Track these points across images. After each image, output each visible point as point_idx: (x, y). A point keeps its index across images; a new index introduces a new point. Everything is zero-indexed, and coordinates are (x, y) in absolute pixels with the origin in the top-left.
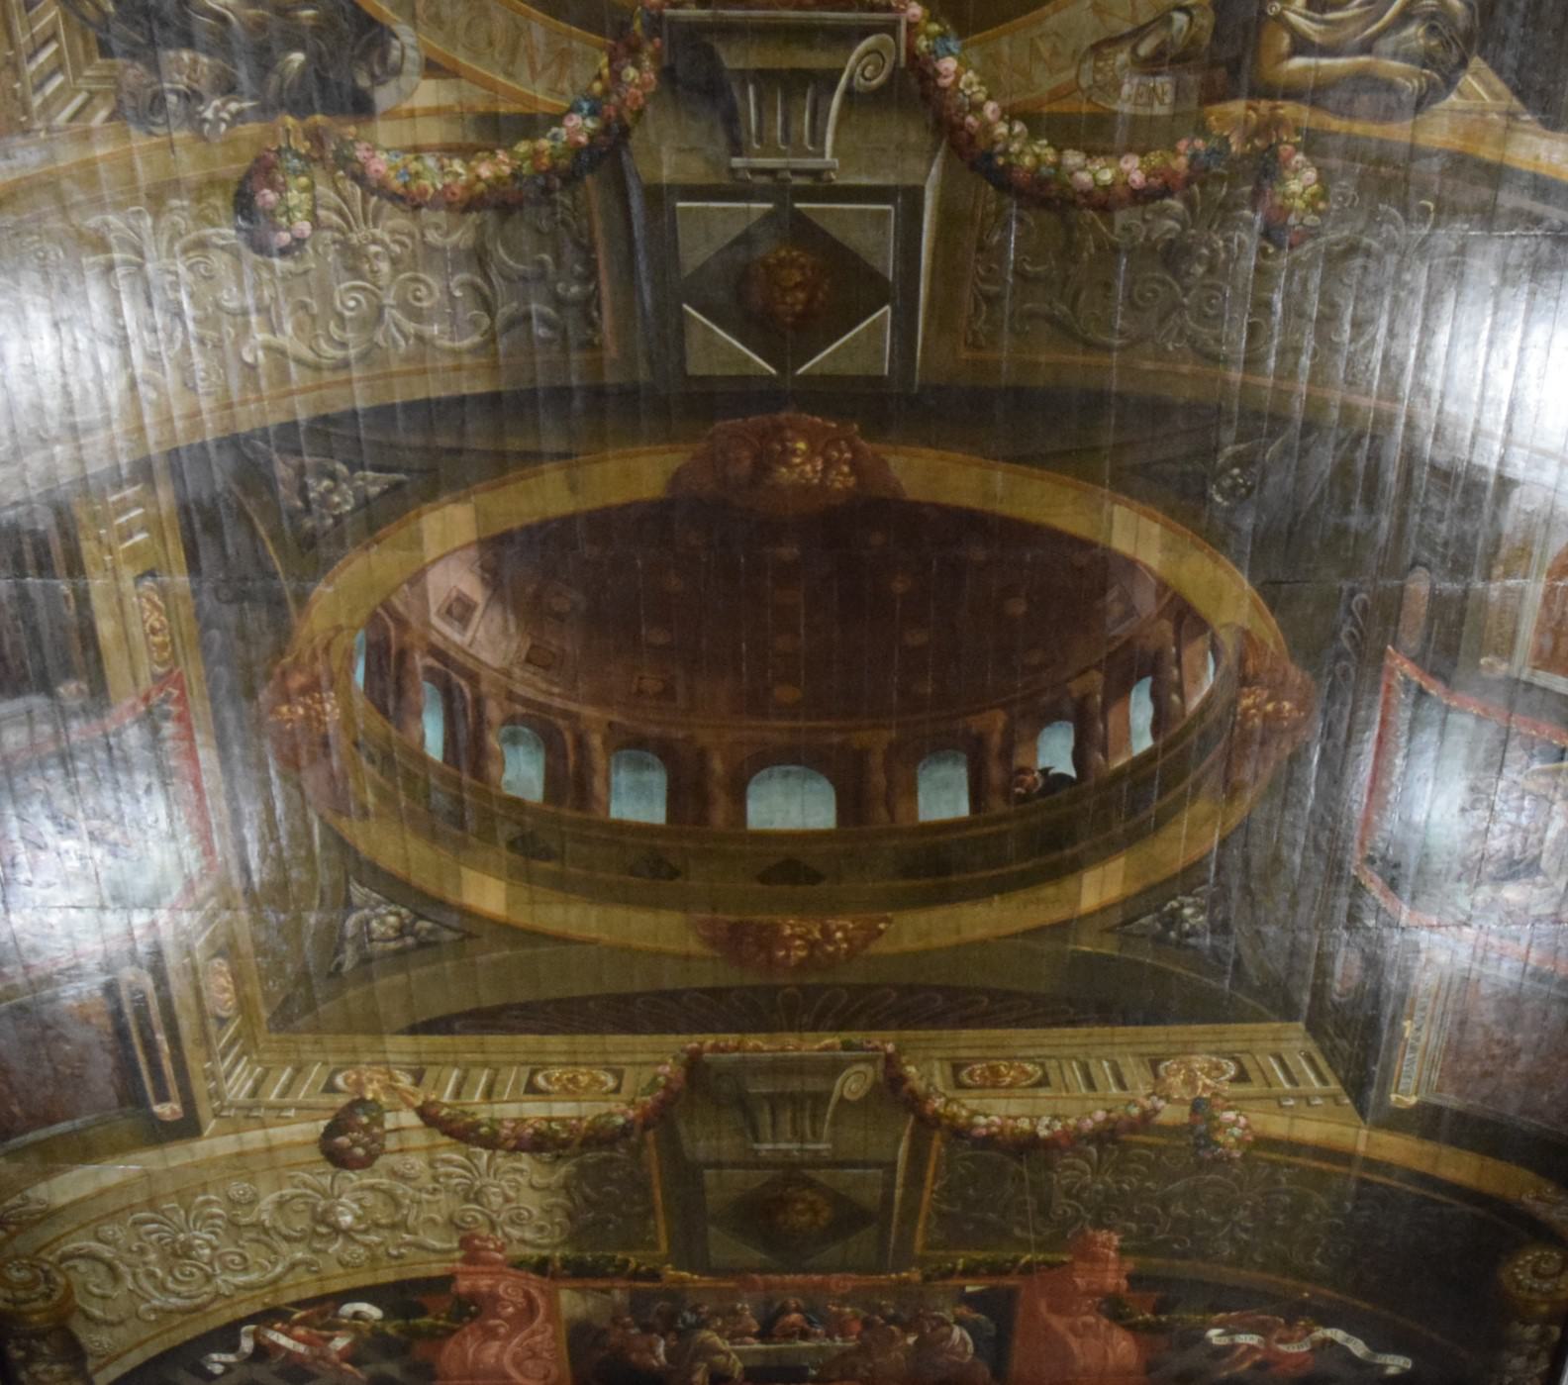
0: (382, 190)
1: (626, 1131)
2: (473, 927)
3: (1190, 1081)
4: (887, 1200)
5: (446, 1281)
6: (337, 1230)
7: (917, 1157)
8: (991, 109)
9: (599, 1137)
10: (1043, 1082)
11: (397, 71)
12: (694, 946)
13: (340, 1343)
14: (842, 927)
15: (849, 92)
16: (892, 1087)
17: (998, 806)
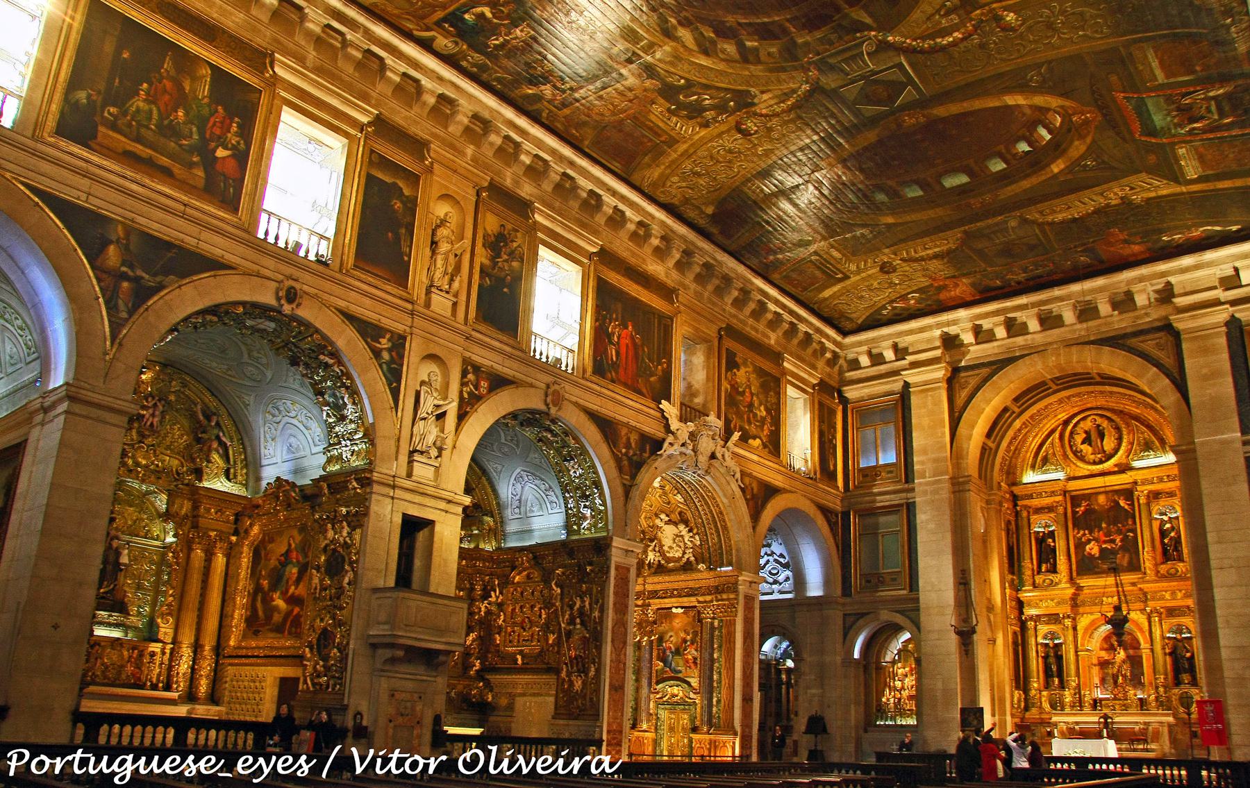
0: (766, 116)
1: (957, 248)
2: (889, 226)
3: (1116, 194)
4: (1040, 240)
5: (931, 285)
6: (896, 284)
7: (1043, 232)
8: (908, 41)
9: (949, 252)
10: (1069, 207)
11: (756, 96)
12: (949, 212)
13: (912, 302)
14: (987, 197)
15: (868, 54)
16: (1024, 221)
17: (1014, 162)
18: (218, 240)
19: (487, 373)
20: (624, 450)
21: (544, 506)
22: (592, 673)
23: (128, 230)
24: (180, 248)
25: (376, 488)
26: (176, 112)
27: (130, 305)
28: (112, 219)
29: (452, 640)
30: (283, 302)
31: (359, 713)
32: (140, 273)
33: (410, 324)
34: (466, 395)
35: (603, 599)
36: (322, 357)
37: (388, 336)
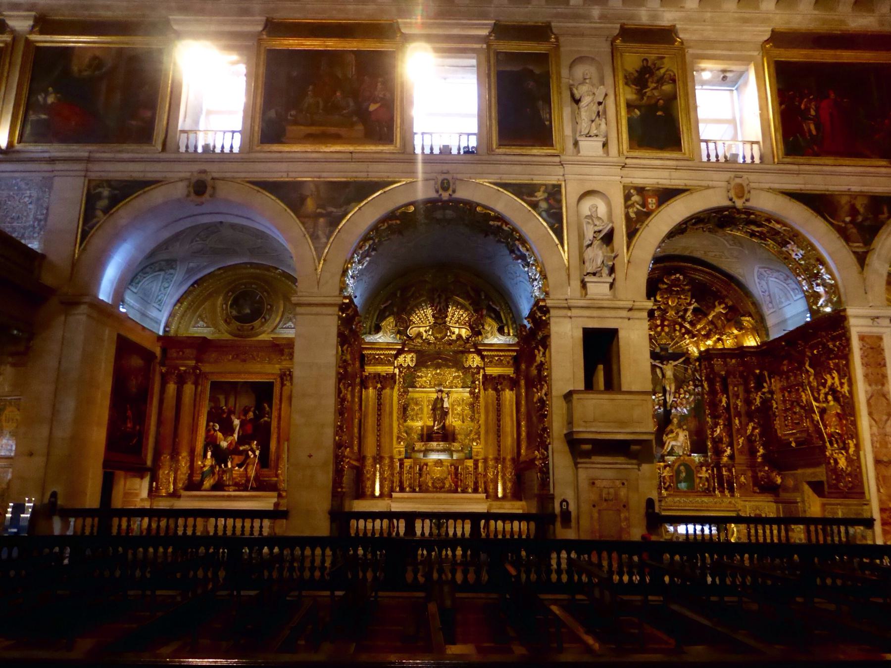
18: (382, 167)
19: (653, 191)
20: (848, 219)
21: (789, 295)
22: (851, 450)
23: (317, 185)
24: (355, 182)
25: (553, 312)
26: (335, 94)
27: (327, 232)
28: (306, 181)
29: (638, 430)
30: (441, 192)
31: (564, 500)
32: (330, 209)
33: (562, 174)
34: (633, 215)
35: (849, 373)
36: (491, 223)
37: (542, 189)
